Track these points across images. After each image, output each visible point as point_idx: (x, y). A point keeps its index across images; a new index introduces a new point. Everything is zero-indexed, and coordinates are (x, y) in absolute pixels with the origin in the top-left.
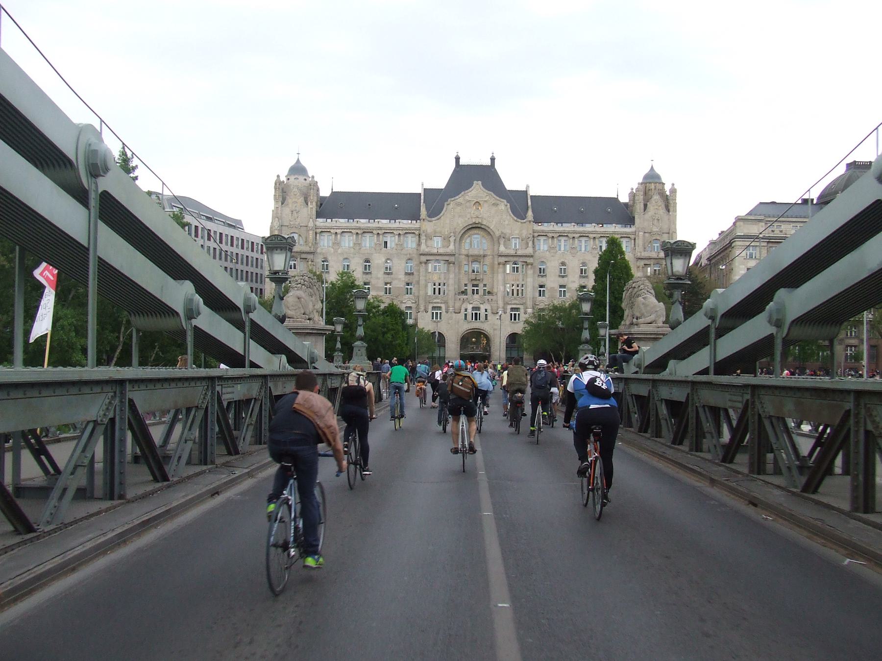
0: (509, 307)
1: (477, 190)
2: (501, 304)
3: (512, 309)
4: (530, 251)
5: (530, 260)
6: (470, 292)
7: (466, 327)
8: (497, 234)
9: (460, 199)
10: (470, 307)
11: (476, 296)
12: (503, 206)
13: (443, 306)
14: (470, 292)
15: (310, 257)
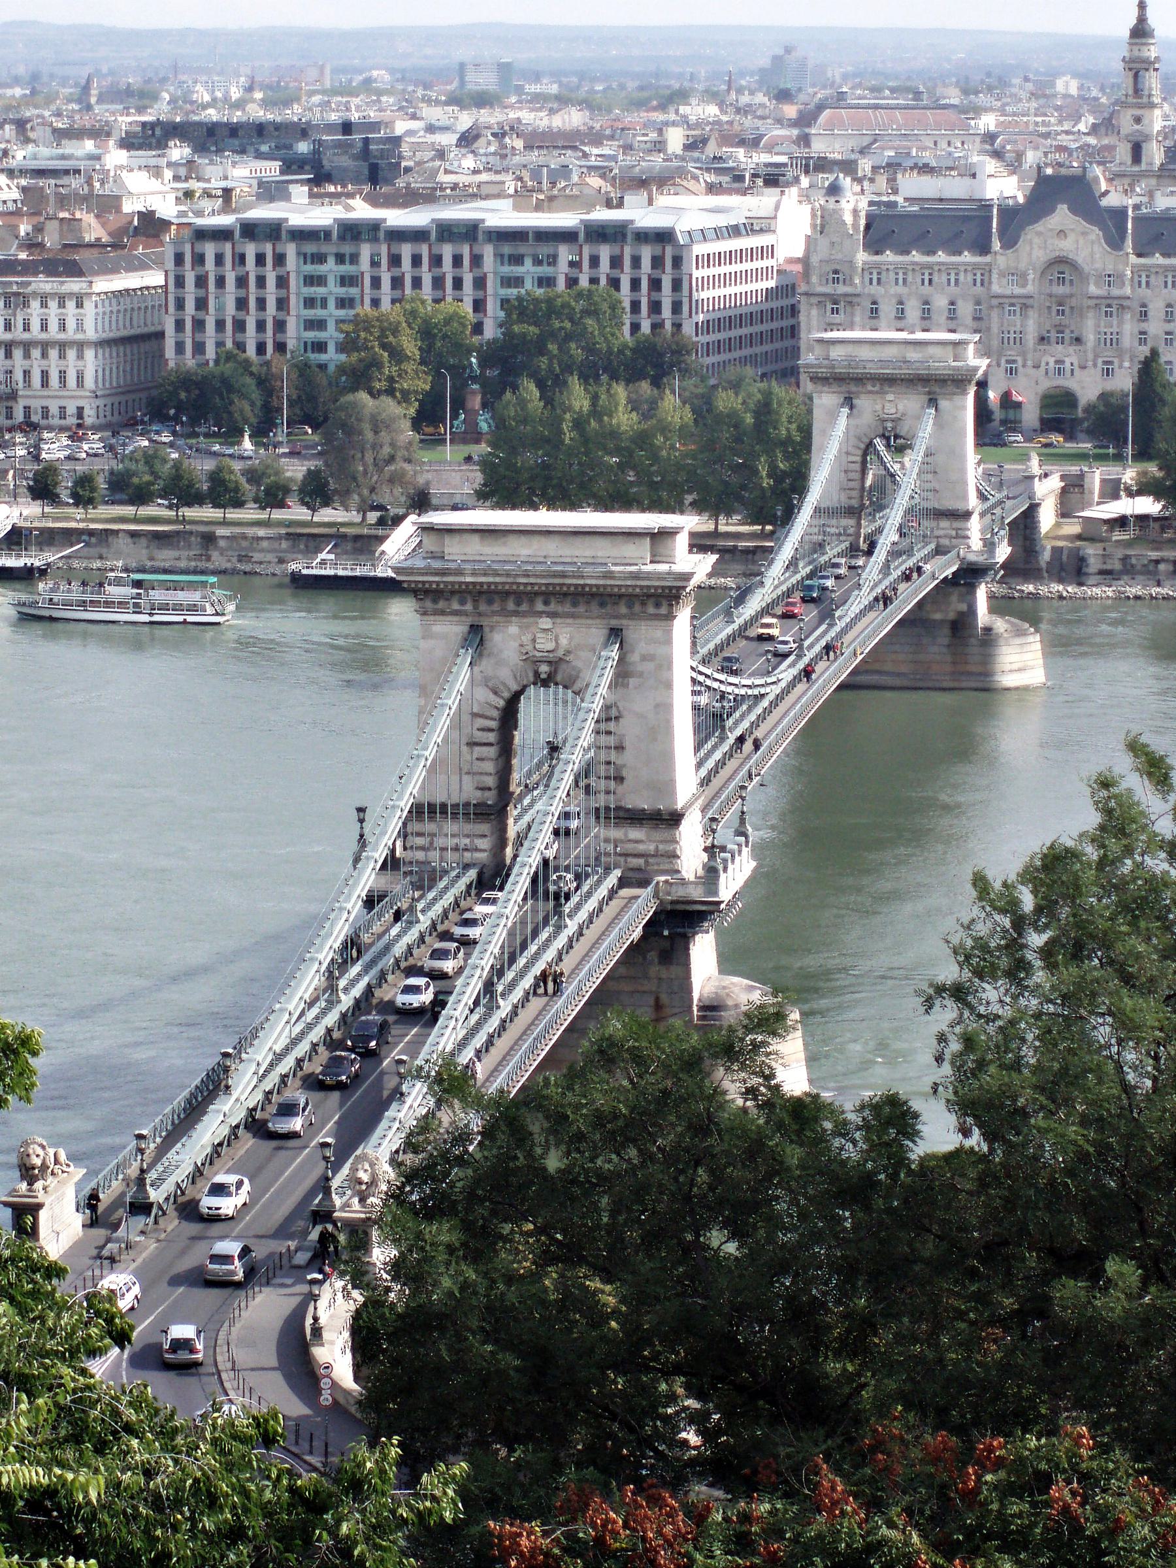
0: (1100, 361)
1: (1062, 216)
2: (1090, 356)
3: (1105, 363)
4: (1128, 291)
5: (1126, 303)
6: (1053, 340)
7: (1046, 384)
8: (1087, 269)
9: (1039, 227)
10: (1052, 364)
11: (1060, 347)
12: (1096, 233)
13: (1020, 359)
14: (1053, 340)
15: (855, 300)
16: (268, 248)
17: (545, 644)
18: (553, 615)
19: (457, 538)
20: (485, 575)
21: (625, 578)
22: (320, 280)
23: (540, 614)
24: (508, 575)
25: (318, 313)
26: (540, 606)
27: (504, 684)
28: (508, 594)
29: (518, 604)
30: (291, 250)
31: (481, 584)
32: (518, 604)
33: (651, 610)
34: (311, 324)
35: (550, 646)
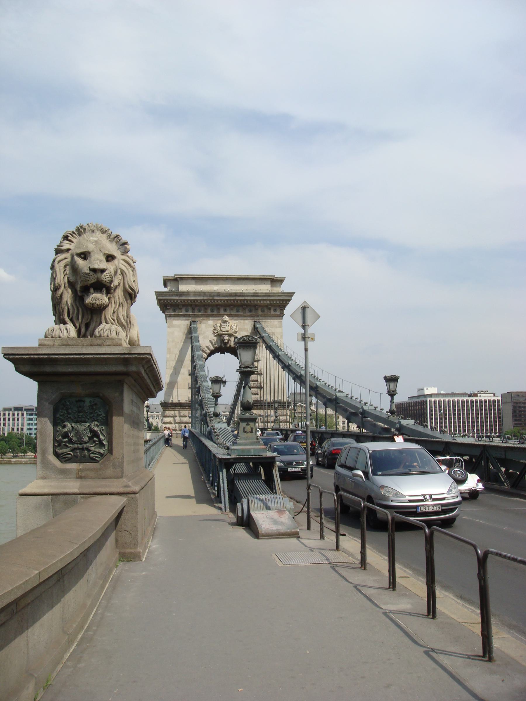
16: (20, 412)
17: (226, 328)
18: (229, 316)
19: (185, 281)
20: (200, 295)
21: (263, 296)
22: (31, 419)
23: (223, 315)
24: (210, 295)
25: (31, 426)
26: (222, 312)
27: (207, 347)
28: (209, 305)
29: (212, 311)
30: (25, 413)
31: (197, 300)
32: (212, 311)
33: (272, 313)
34: (29, 429)
35: (228, 328)
